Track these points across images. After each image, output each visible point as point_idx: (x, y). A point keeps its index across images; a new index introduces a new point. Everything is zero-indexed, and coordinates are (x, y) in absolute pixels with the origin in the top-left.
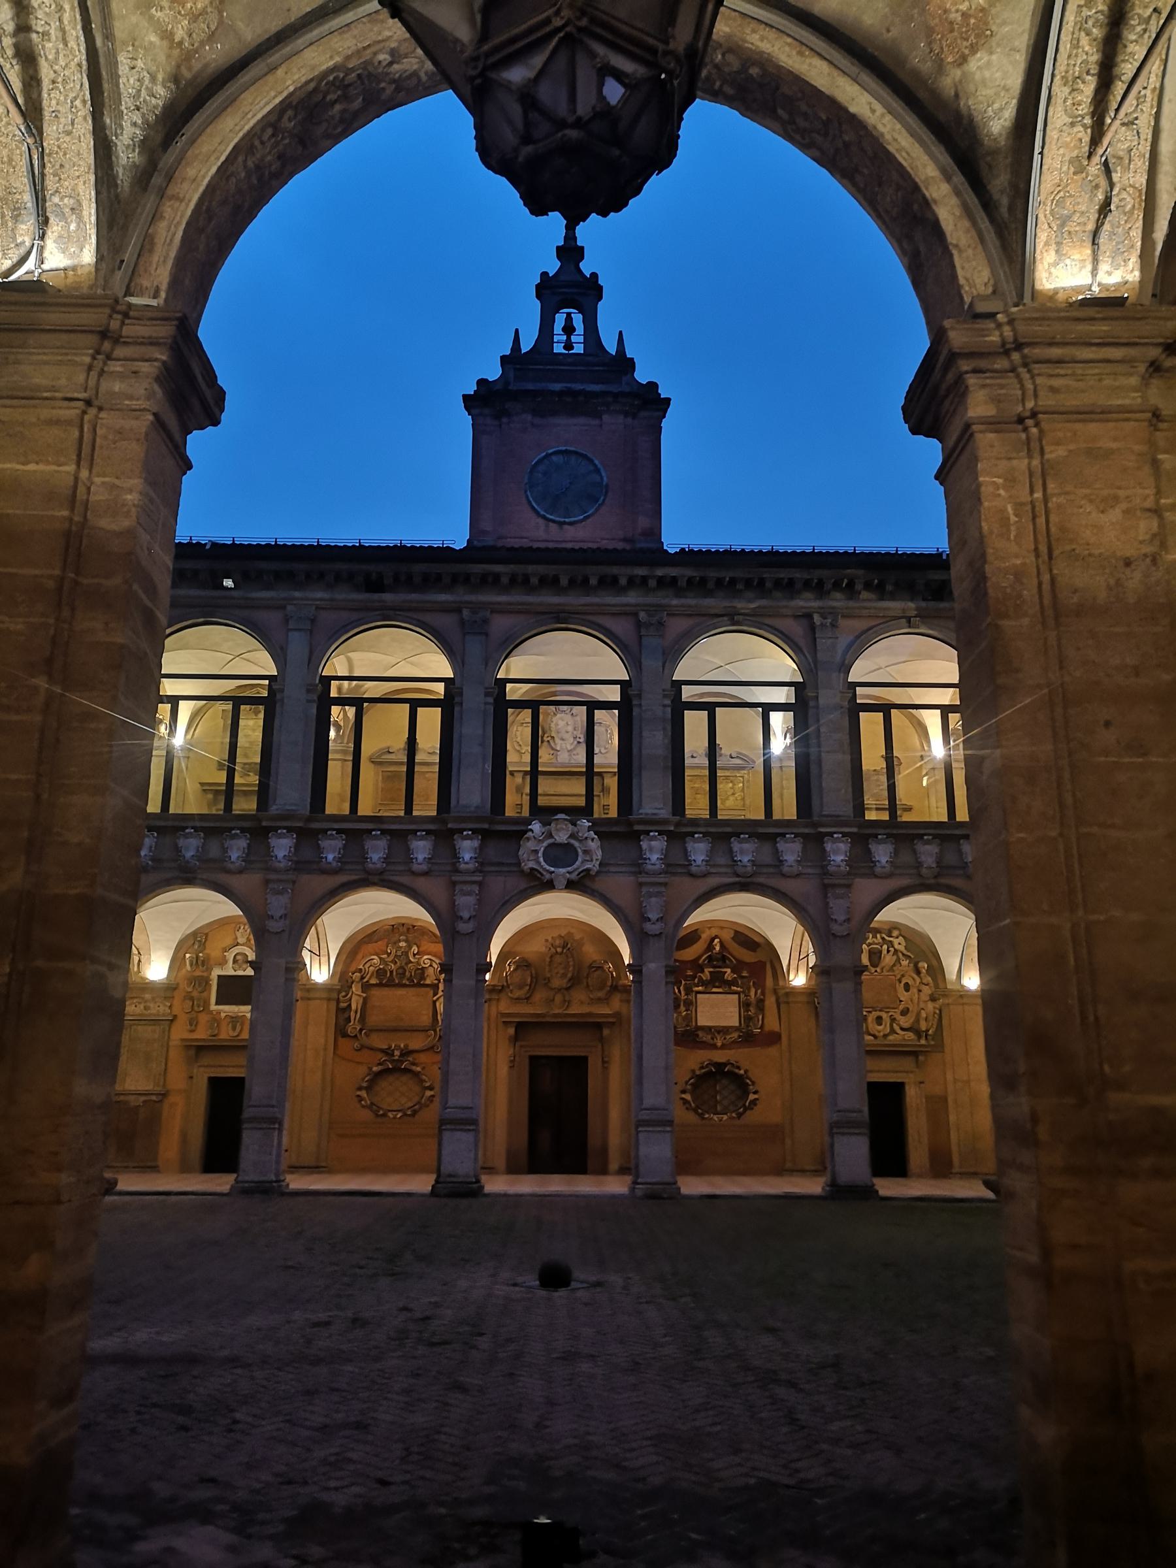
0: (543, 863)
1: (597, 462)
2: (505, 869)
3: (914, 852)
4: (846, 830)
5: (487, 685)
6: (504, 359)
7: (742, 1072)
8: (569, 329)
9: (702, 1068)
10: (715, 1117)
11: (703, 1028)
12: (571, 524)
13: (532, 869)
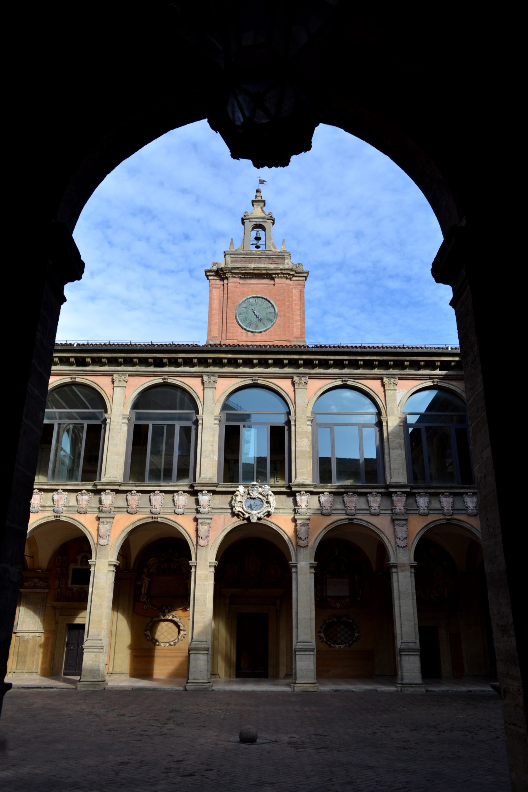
0: (245, 508)
1: (272, 302)
3: (440, 501)
5: (215, 414)
6: (225, 254)
7: (351, 621)
8: (258, 239)
9: (329, 619)
10: (337, 646)
13: (239, 511)
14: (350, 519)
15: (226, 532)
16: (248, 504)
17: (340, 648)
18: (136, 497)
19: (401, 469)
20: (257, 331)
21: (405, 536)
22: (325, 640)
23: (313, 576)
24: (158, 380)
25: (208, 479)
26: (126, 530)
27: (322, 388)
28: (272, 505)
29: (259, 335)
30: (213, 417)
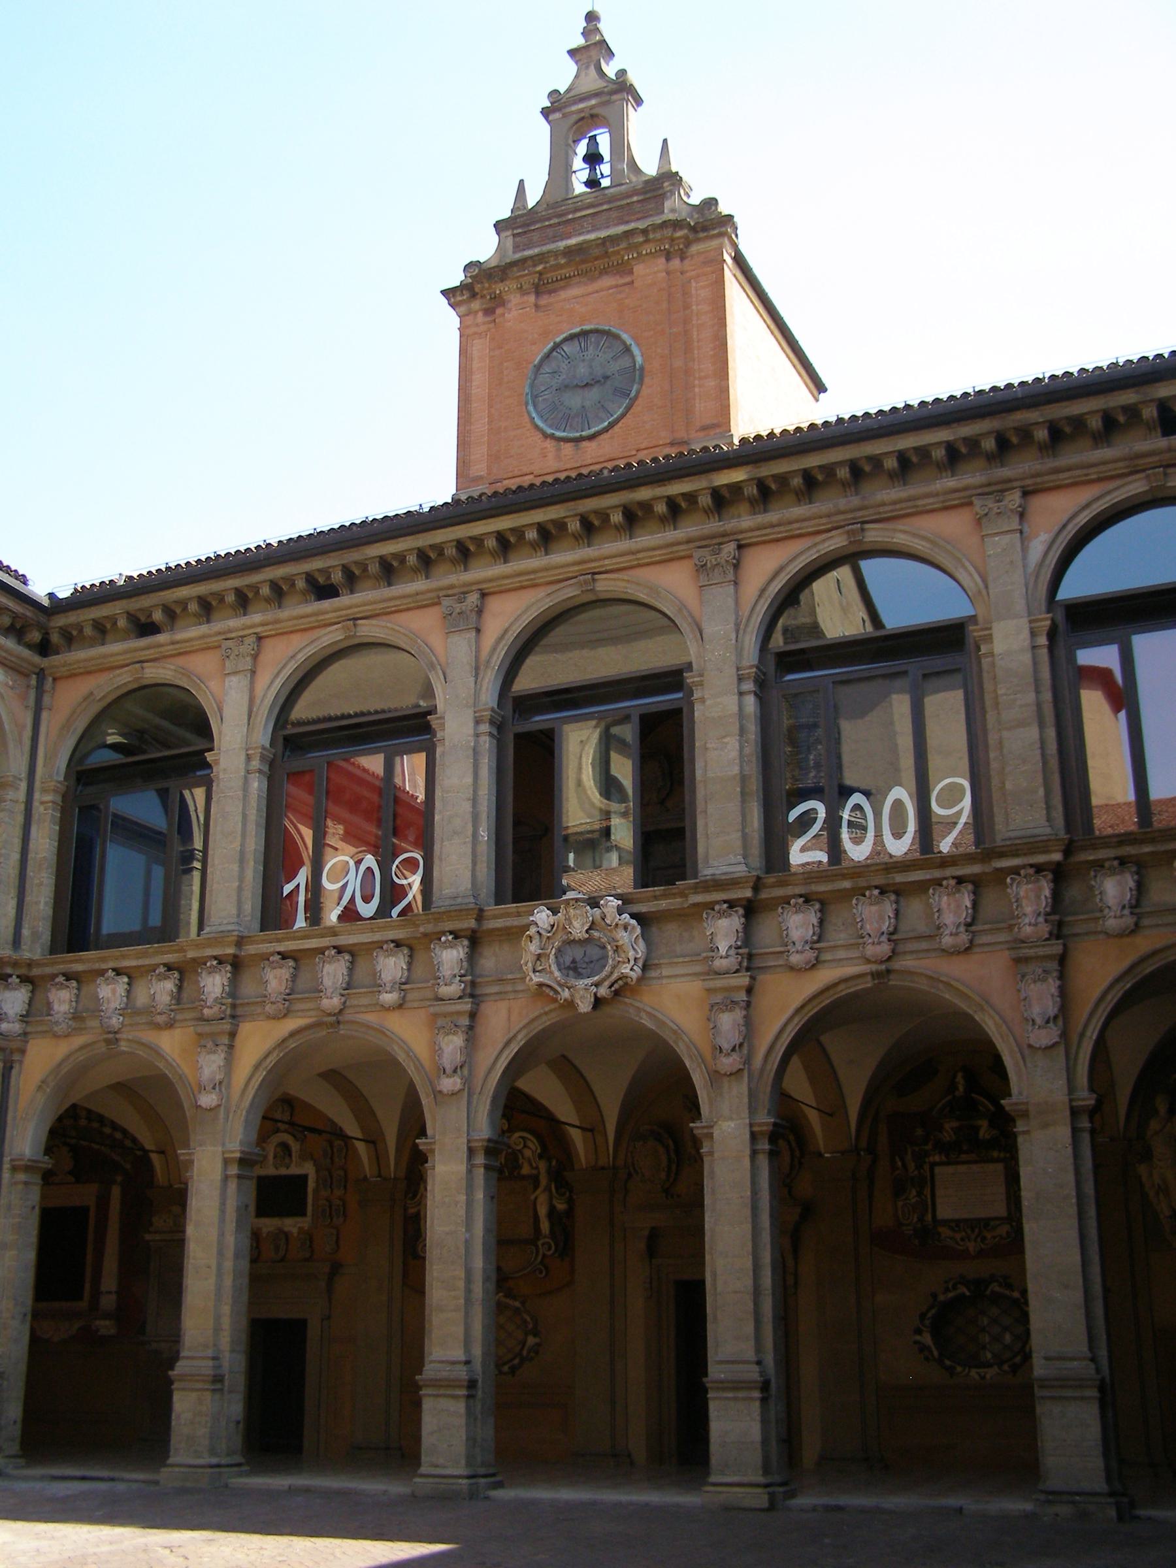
1: (625, 336)
2: (509, 988)
4: (1040, 859)
6: (499, 226)
8: (593, 158)
9: (947, 1290)
10: (974, 1373)
11: (945, 1223)
12: (591, 438)
13: (541, 985)
14: (876, 975)
15: (514, 1048)
16: (568, 960)
17: (983, 1378)
18: (283, 971)
19: (1041, 792)
20: (584, 433)
21: (1052, 1010)
22: (936, 1353)
23: (764, 1162)
24: (332, 637)
25: (459, 900)
26: (265, 1064)
27: (781, 569)
28: (631, 954)
29: (593, 445)
30: (468, 716)
